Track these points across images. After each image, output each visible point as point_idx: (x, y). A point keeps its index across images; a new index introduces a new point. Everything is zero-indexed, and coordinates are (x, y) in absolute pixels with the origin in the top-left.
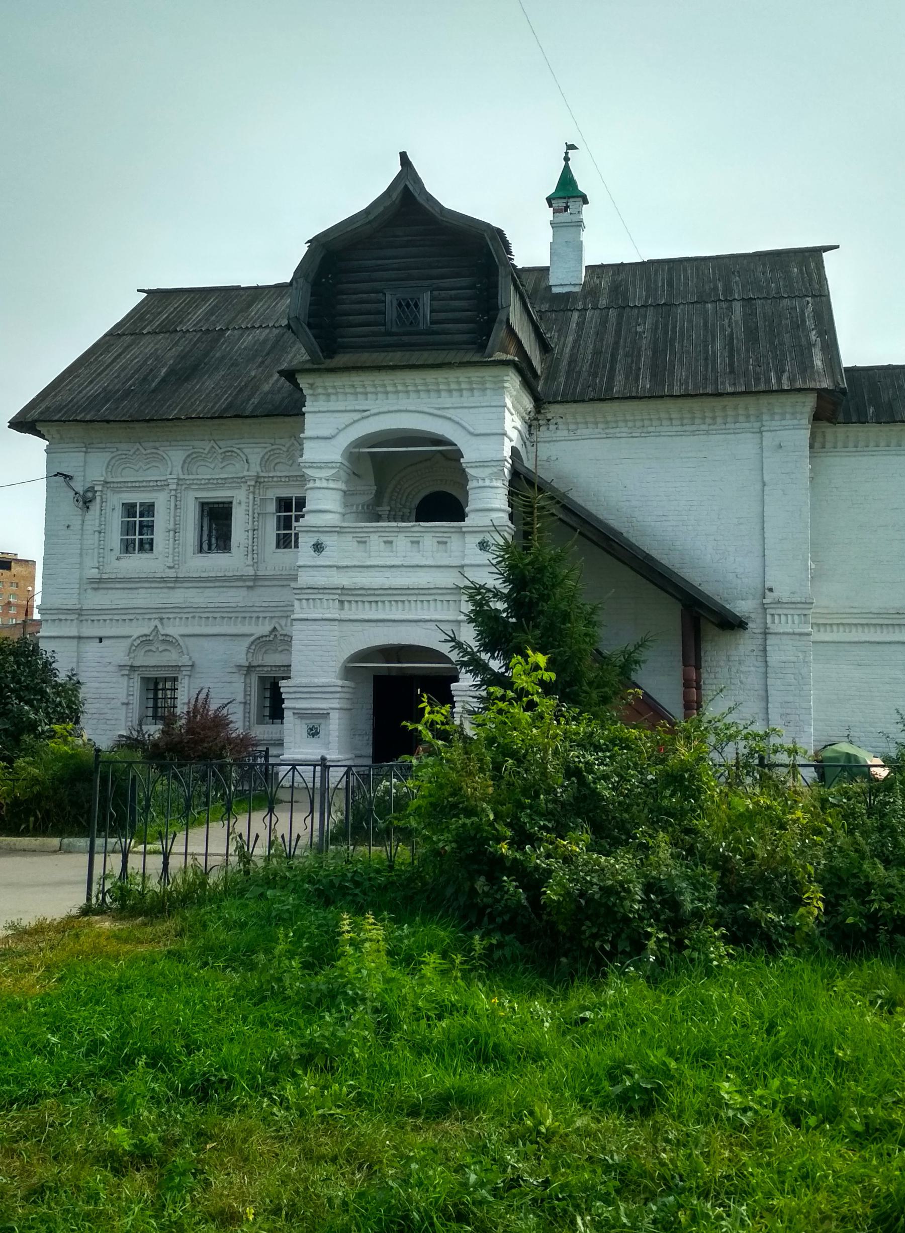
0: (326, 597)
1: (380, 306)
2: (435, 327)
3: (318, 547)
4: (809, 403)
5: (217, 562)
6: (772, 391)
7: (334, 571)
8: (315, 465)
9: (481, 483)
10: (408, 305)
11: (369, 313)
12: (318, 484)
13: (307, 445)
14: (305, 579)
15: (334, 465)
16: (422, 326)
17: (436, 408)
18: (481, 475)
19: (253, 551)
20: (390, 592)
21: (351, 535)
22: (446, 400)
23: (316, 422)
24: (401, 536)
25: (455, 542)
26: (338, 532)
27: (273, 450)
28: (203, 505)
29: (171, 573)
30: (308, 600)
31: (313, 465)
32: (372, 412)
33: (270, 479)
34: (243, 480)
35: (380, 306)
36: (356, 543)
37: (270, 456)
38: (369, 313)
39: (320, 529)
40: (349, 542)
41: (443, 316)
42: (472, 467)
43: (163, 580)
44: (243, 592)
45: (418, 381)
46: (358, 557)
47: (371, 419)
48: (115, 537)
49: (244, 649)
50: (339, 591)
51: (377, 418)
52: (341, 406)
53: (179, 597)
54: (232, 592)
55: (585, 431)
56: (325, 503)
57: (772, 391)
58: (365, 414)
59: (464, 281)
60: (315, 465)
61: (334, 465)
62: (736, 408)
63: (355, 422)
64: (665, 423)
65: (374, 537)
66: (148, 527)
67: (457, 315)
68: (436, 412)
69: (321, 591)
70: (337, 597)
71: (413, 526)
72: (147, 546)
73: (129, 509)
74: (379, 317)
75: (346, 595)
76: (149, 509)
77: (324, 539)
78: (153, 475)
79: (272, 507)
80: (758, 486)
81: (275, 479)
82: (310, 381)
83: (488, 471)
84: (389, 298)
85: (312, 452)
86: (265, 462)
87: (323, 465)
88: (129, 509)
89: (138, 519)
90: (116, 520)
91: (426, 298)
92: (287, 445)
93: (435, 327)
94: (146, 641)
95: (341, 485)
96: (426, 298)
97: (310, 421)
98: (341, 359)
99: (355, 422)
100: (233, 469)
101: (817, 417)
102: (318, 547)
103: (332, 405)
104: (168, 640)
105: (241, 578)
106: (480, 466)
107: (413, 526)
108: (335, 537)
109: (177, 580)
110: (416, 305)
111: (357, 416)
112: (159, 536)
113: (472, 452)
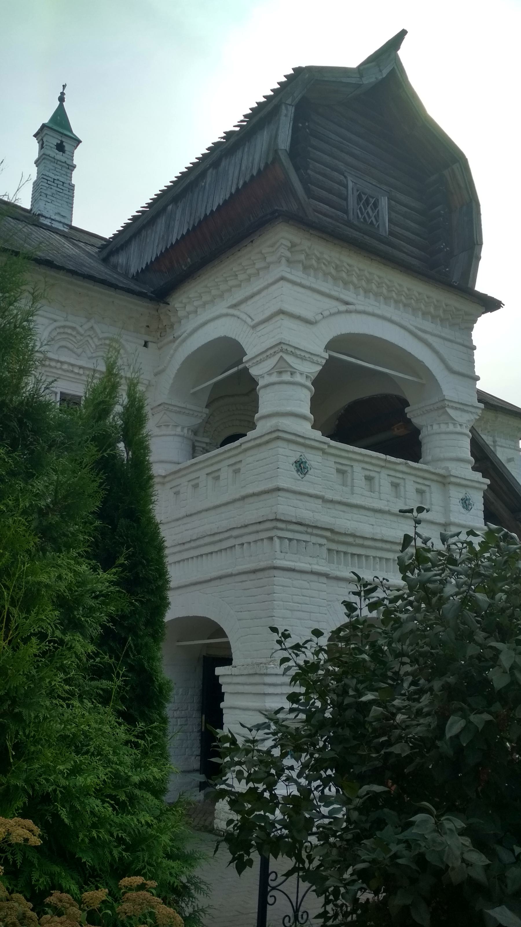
0: (314, 539)
3: (301, 467)
7: (317, 505)
8: (298, 352)
10: (367, 202)
12: (298, 378)
15: (320, 360)
17: (416, 328)
18: (460, 420)
20: (379, 545)
21: (333, 459)
24: (384, 472)
26: (324, 452)
27: (64, 327)
30: (290, 540)
32: (360, 308)
33: (59, 365)
36: (334, 471)
37: (58, 333)
39: (308, 442)
42: (452, 407)
47: (354, 316)
50: (328, 534)
51: (359, 316)
52: (325, 286)
58: (348, 308)
60: (298, 352)
61: (320, 360)
63: (339, 312)
65: (357, 467)
68: (420, 333)
69: (310, 530)
70: (323, 541)
71: (399, 464)
81: (65, 367)
82: (297, 240)
87: (307, 356)
92: (86, 327)
99: (339, 312)
102: (301, 467)
103: (310, 281)
106: (460, 409)
107: (399, 464)
111: (343, 308)
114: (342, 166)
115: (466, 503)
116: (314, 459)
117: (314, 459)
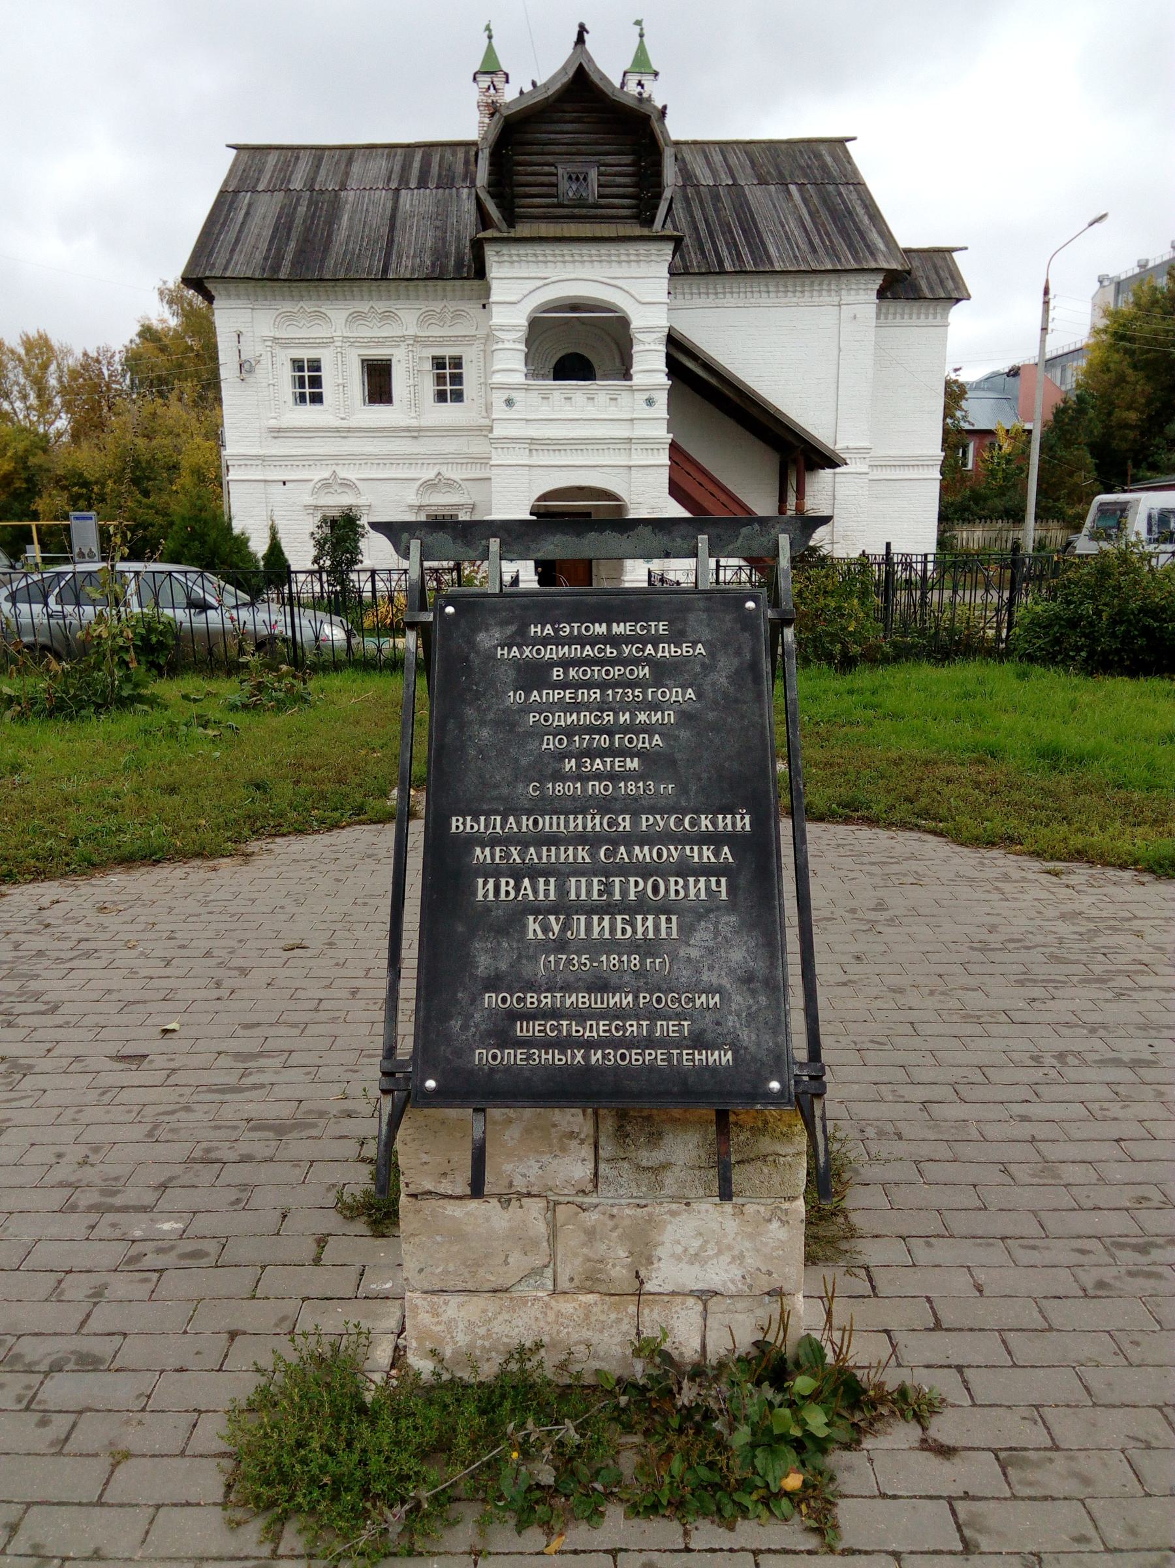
1: (553, 179)
2: (603, 201)
3: (509, 402)
4: (877, 281)
5: (379, 415)
6: (746, 272)
9: (647, 347)
10: (577, 179)
11: (542, 185)
13: (495, 309)
14: (498, 431)
16: (591, 200)
19: (415, 403)
22: (617, 270)
23: (499, 290)
24: (579, 393)
25: (625, 398)
28: (363, 361)
29: (344, 424)
31: (502, 328)
34: (404, 338)
35: (553, 179)
38: (542, 185)
40: (534, 397)
41: (608, 191)
43: (337, 430)
44: (409, 441)
45: (594, 252)
46: (545, 411)
48: (287, 389)
49: (414, 490)
53: (353, 446)
54: (398, 441)
55: (828, 299)
56: (510, 362)
57: (746, 272)
59: (627, 159)
62: (777, 286)
64: (764, 295)
65: (556, 394)
66: (457, 379)
67: (621, 190)
72: (317, 399)
73: (298, 365)
74: (553, 190)
75: (534, 444)
76: (315, 365)
77: (515, 395)
78: (320, 331)
79: (428, 365)
80: (836, 352)
83: (654, 336)
84: (560, 171)
85: (499, 316)
86: (422, 322)
88: (298, 365)
89: (306, 374)
90: (287, 374)
91: (593, 174)
93: (603, 201)
94: (326, 484)
95: (523, 347)
96: (593, 174)
97: (495, 286)
98: (522, 230)
100: (405, 330)
101: (881, 294)
102: (509, 402)
104: (347, 484)
105: (408, 429)
108: (522, 394)
109: (349, 430)
110: (585, 179)
111: (541, 283)
112: (327, 389)
113: (637, 321)
114: (550, 158)
115: (650, 402)
116: (517, 396)
117: (517, 396)
